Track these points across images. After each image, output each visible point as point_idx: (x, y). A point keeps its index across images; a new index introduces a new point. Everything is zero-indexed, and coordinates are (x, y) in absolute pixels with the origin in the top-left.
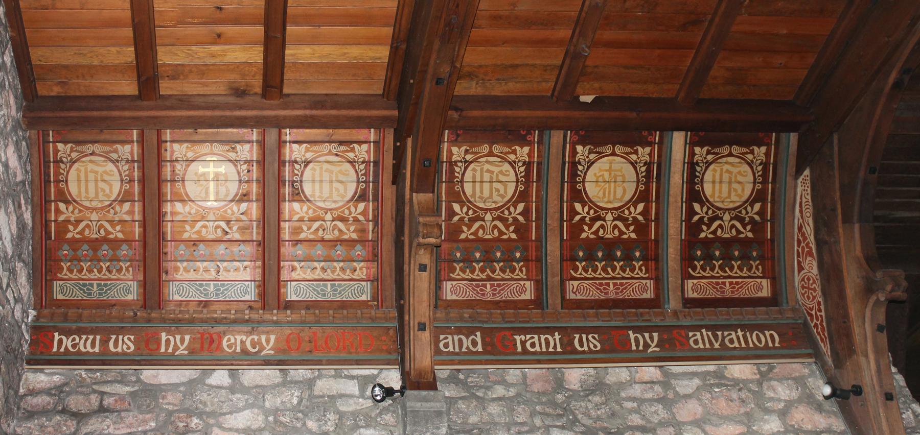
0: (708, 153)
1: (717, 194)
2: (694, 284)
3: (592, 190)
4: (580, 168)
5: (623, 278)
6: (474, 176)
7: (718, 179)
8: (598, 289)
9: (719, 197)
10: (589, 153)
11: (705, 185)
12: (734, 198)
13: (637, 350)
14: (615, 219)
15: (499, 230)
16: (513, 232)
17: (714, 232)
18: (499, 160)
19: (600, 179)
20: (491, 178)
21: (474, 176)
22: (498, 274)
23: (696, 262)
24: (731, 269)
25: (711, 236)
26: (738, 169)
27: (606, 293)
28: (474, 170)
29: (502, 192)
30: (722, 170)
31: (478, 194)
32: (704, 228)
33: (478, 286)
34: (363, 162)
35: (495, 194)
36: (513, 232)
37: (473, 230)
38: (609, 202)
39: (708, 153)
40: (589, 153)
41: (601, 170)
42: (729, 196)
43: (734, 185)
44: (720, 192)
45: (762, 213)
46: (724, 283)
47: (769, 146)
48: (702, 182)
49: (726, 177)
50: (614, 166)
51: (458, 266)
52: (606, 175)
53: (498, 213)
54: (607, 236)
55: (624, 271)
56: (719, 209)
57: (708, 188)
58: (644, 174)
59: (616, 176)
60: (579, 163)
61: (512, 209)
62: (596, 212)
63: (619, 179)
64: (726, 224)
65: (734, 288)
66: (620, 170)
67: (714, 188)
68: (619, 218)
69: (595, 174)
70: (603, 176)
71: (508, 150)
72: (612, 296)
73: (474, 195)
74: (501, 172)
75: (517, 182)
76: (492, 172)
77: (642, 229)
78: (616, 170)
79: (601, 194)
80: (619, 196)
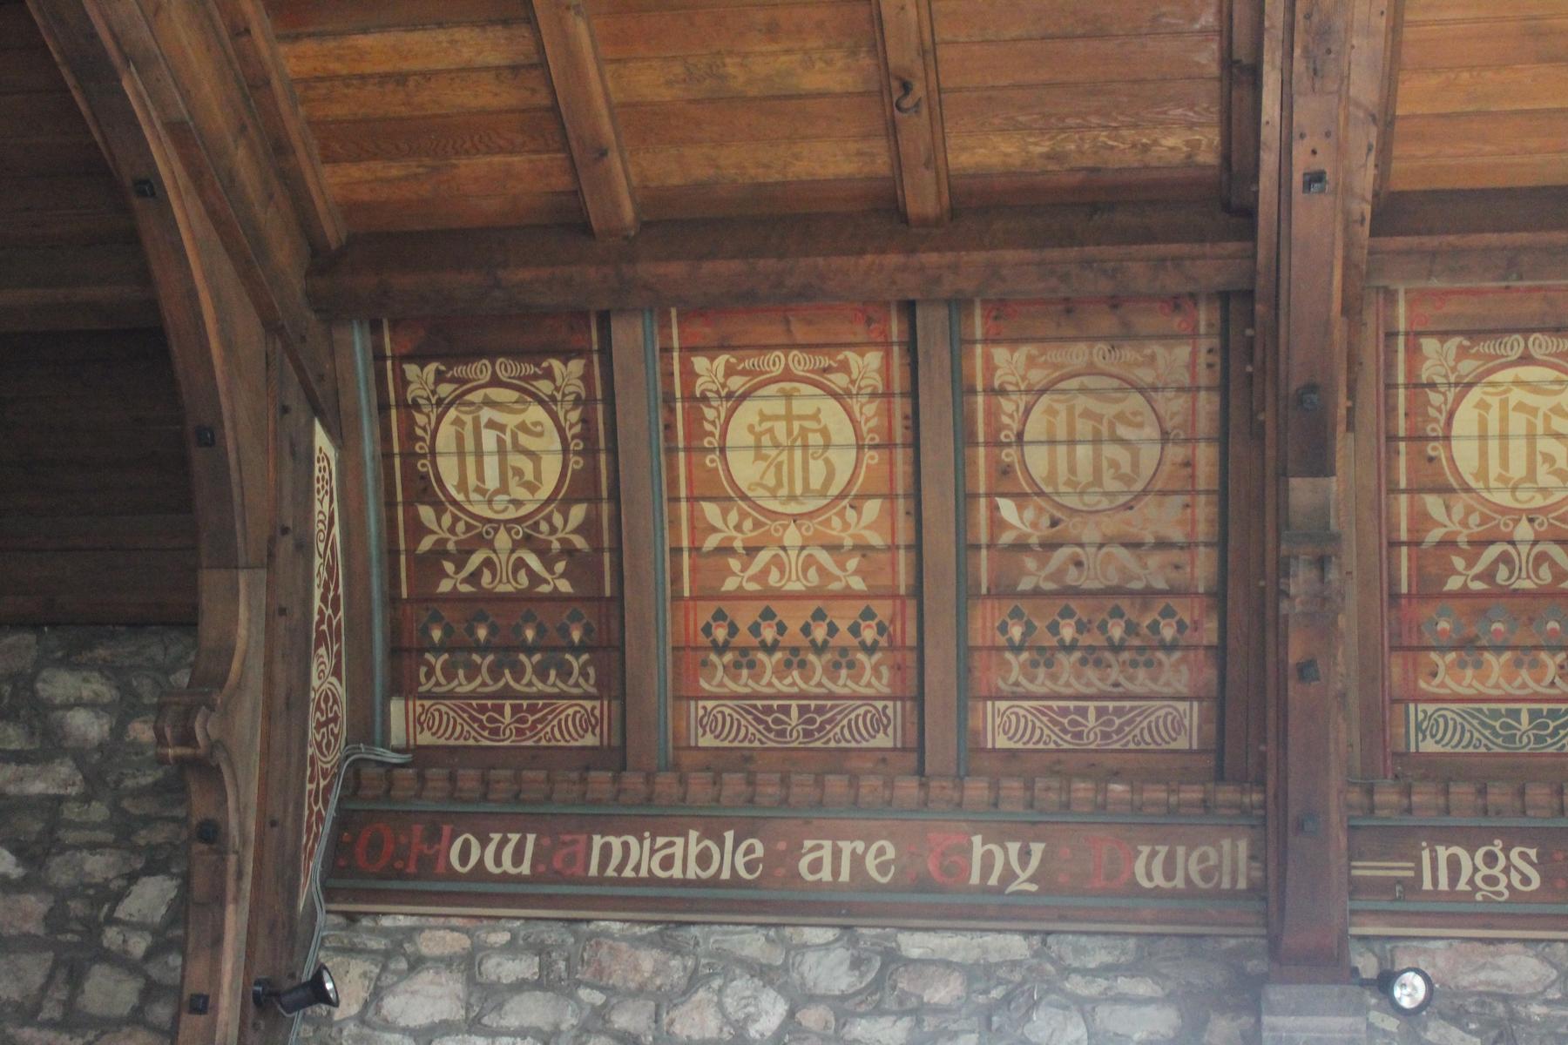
1: (1494, 468)
3: (744, 469)
4: (1435, 398)
5: (831, 696)
6: (460, 439)
7: (1061, 434)
8: (1055, 723)
9: (1501, 478)
10: (1458, 359)
11: (440, 461)
12: (1111, 484)
13: (1435, 893)
14: (516, 545)
15: (531, 573)
16: (562, 576)
18: (515, 395)
19: (766, 440)
20: (500, 441)
21: (460, 439)
22: (530, 682)
23: (522, 657)
24: (518, 674)
25: (465, 588)
27: (1078, 735)
28: (458, 422)
29: (529, 475)
30: (476, 422)
31: (472, 480)
32: (449, 567)
33: (483, 709)
34: (873, 395)
35: (513, 482)
36: (562, 576)
37: (755, 568)
38: (792, 497)
40: (1458, 359)
41: (764, 418)
42: (504, 488)
44: (1504, 462)
45: (588, 528)
47: (886, 345)
48: (433, 453)
49: (1518, 423)
50: (799, 407)
51: (439, 662)
52: (780, 428)
53: (813, 525)
54: (502, 588)
55: (834, 679)
56: (1504, 510)
57: (1465, 454)
58: (577, 429)
59: (804, 431)
60: (416, 406)
61: (558, 519)
62: (1485, 519)
63: (815, 439)
64: (503, 559)
65: (812, 721)
66: (815, 417)
67: (1483, 454)
68: (528, 541)
69: (751, 428)
70: (770, 431)
71: (532, 369)
72: (1092, 742)
73: (1052, 476)
74: (523, 427)
75: (565, 450)
76: (501, 428)
77: (581, 565)
78: (800, 418)
79: (771, 481)
80: (816, 482)
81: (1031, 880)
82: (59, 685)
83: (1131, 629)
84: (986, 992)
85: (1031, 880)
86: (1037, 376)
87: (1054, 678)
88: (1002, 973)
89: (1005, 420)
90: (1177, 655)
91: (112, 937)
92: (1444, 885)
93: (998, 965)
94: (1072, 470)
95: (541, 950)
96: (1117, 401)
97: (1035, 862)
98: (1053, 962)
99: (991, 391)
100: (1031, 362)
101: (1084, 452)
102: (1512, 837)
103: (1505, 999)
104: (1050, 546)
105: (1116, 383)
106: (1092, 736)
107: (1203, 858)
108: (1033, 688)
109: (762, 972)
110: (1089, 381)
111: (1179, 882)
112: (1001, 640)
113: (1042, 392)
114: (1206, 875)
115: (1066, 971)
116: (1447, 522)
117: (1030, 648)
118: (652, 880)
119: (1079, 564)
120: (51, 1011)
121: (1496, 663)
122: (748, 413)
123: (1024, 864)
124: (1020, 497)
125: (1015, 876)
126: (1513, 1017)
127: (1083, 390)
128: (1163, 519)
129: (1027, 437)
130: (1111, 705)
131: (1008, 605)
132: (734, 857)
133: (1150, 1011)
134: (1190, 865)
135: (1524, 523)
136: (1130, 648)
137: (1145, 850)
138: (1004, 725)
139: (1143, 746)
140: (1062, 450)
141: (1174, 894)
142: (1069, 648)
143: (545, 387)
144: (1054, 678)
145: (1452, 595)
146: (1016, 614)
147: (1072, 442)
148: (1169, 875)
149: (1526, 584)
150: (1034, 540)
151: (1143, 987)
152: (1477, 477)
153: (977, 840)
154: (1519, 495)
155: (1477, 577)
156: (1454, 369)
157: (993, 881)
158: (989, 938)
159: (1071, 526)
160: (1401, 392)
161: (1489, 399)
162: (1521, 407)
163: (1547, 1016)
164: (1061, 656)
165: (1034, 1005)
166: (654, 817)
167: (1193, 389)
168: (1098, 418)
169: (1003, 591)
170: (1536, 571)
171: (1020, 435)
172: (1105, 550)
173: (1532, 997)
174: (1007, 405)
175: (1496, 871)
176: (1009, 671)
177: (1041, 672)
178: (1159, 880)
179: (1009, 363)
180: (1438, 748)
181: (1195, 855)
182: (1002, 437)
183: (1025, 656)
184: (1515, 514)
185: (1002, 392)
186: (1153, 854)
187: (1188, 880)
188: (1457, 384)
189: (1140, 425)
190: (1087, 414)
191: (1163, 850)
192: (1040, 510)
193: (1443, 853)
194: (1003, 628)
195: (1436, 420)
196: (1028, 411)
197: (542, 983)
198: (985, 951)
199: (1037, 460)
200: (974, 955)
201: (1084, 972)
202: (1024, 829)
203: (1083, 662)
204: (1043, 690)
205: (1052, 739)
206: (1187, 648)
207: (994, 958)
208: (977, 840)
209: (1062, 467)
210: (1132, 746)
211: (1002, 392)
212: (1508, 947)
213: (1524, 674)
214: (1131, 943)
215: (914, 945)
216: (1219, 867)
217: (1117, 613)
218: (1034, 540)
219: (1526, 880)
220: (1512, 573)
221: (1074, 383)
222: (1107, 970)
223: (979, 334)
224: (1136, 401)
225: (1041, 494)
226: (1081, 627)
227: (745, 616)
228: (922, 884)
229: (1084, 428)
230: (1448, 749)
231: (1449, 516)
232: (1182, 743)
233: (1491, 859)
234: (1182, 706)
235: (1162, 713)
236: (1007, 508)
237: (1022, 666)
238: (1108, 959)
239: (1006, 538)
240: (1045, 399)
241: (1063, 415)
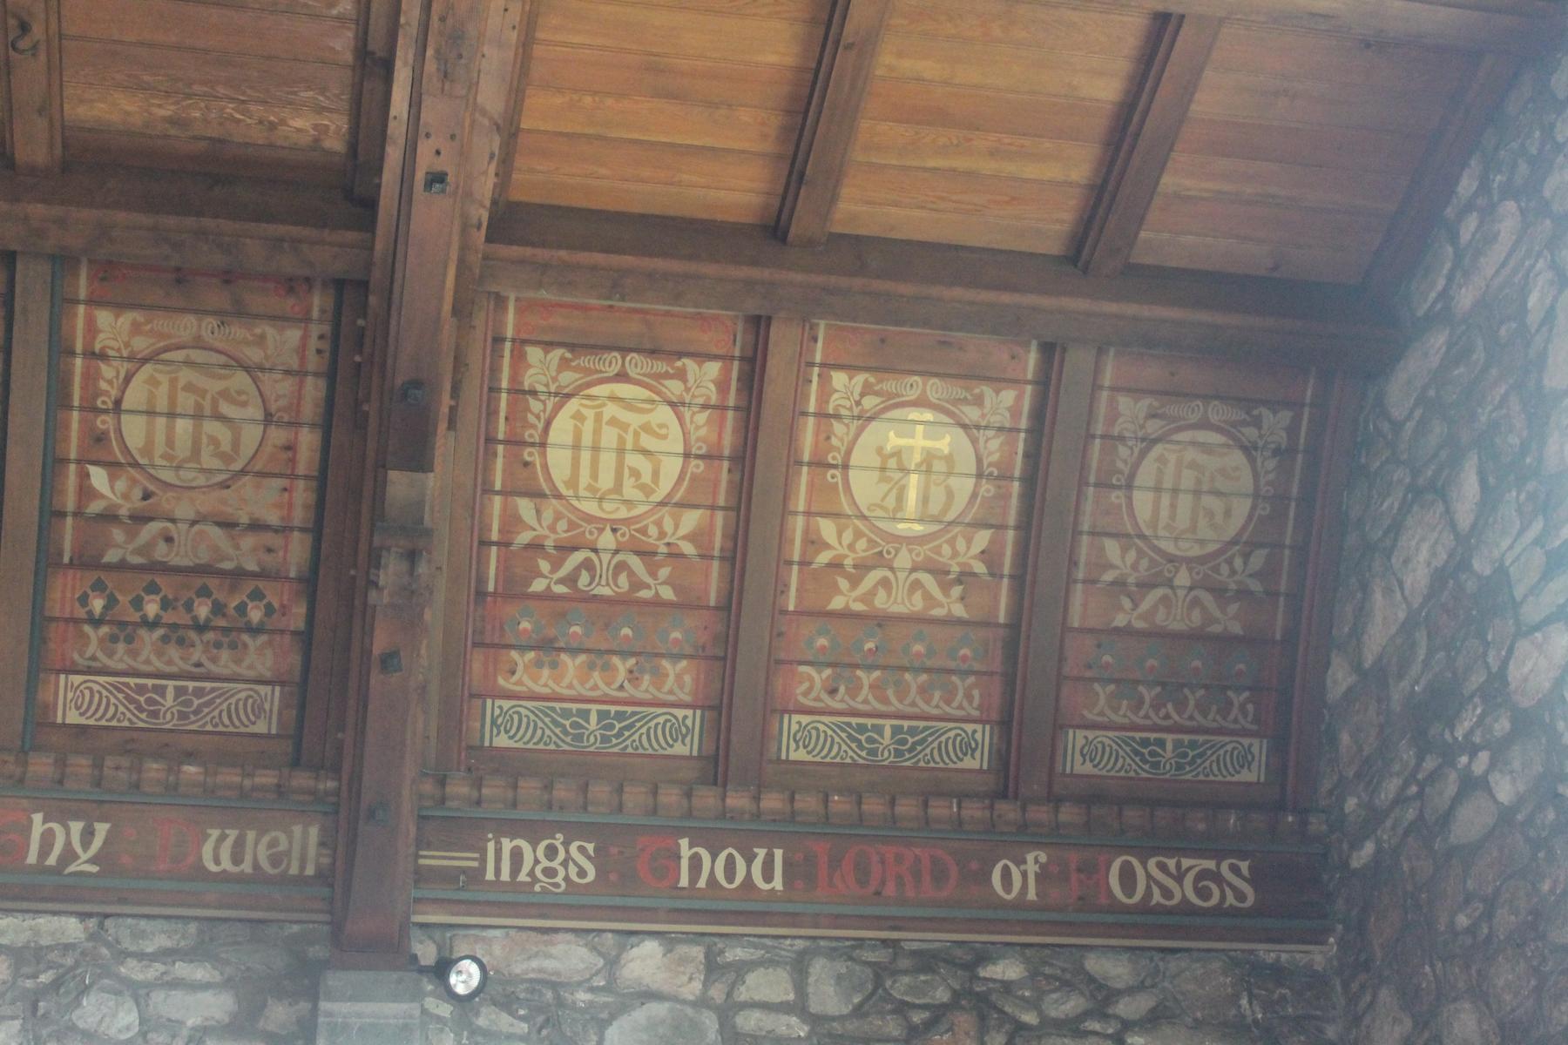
0: (867, 390)
2: (503, 713)
4: (535, 405)
7: (162, 405)
9: (590, 488)
10: (560, 370)
13: (498, 882)
17: (868, 598)
26: (644, 418)
39: (867, 390)
40: (560, 370)
43: (633, 460)
46: (879, 730)
49: (609, 437)
56: (590, 519)
57: (558, 461)
62: (572, 526)
81: (91, 861)
83: (218, 609)
84: (35, 976)
85: (91, 861)
86: (141, 344)
87: (134, 654)
88: (53, 956)
89: (103, 385)
90: (264, 638)
92: (505, 876)
93: (50, 948)
94: (170, 442)
96: (221, 377)
97: (97, 843)
98: (108, 945)
99: (90, 354)
100: (136, 329)
101: (183, 426)
102: (574, 831)
103: (554, 986)
104: (140, 519)
105: (223, 359)
106: (169, 716)
107: (273, 844)
108: (112, 664)
110: (197, 355)
111: (247, 867)
112: (81, 613)
113: (145, 361)
114: (275, 861)
115: (124, 955)
116: (537, 526)
117: (110, 622)
119: (169, 539)
121: (572, 665)
123: (86, 844)
124: (112, 466)
125: (76, 857)
126: (560, 1003)
127: (189, 363)
129: (125, 406)
130: (191, 685)
131: (94, 576)
133: (207, 997)
134: (259, 850)
135: (608, 533)
136: (215, 628)
137: (215, 833)
138: (74, 700)
139: (220, 728)
140: (161, 422)
141: (240, 879)
142: (153, 625)
144: (134, 654)
145: (537, 597)
146: (99, 586)
147: (172, 415)
148: (237, 859)
149: (606, 591)
150: (123, 512)
151: (201, 973)
152: (568, 484)
153: (38, 818)
154: (607, 506)
155: (561, 581)
156: (555, 379)
157: (52, 860)
158: (42, 921)
159: (165, 501)
160: (504, 396)
161: (584, 411)
162: (613, 422)
163: (591, 1004)
164: (143, 632)
165: (84, 990)
167: (301, 373)
168: (202, 393)
169: (87, 561)
170: (616, 575)
171: (118, 403)
172: (197, 527)
173: (579, 984)
174: (107, 371)
175: (555, 864)
176: (87, 645)
177: (121, 647)
178: (226, 864)
179: (112, 328)
180: (511, 744)
181: (266, 839)
182: (99, 403)
183: (105, 630)
184: (599, 523)
185: (103, 356)
186: (223, 838)
187: (256, 866)
188: (556, 394)
189: (244, 404)
190: (189, 387)
191: (233, 834)
192: (134, 481)
193: (507, 845)
194: (84, 600)
195: (534, 427)
196: (128, 379)
198: (36, 932)
199: (134, 430)
200: (21, 939)
201: (140, 956)
202: (88, 810)
203: (165, 639)
204: (121, 666)
205: (127, 717)
206: (273, 632)
207: (45, 941)
208: (38, 818)
209: (160, 438)
210: (209, 728)
211: (103, 356)
212: (560, 936)
213: (596, 676)
214: (192, 928)
216: (288, 853)
217: (204, 592)
218: (123, 512)
219: (582, 873)
220: (593, 578)
221: (178, 355)
223: (83, 293)
224: (241, 380)
225: (136, 465)
226: (166, 604)
229: (186, 402)
230: (520, 745)
231: (539, 520)
232: (261, 727)
233: (551, 852)
234: (264, 690)
235: (243, 695)
236: (99, 477)
237: (101, 641)
238: (169, 944)
239: (95, 507)
240: (148, 368)
241: (164, 389)
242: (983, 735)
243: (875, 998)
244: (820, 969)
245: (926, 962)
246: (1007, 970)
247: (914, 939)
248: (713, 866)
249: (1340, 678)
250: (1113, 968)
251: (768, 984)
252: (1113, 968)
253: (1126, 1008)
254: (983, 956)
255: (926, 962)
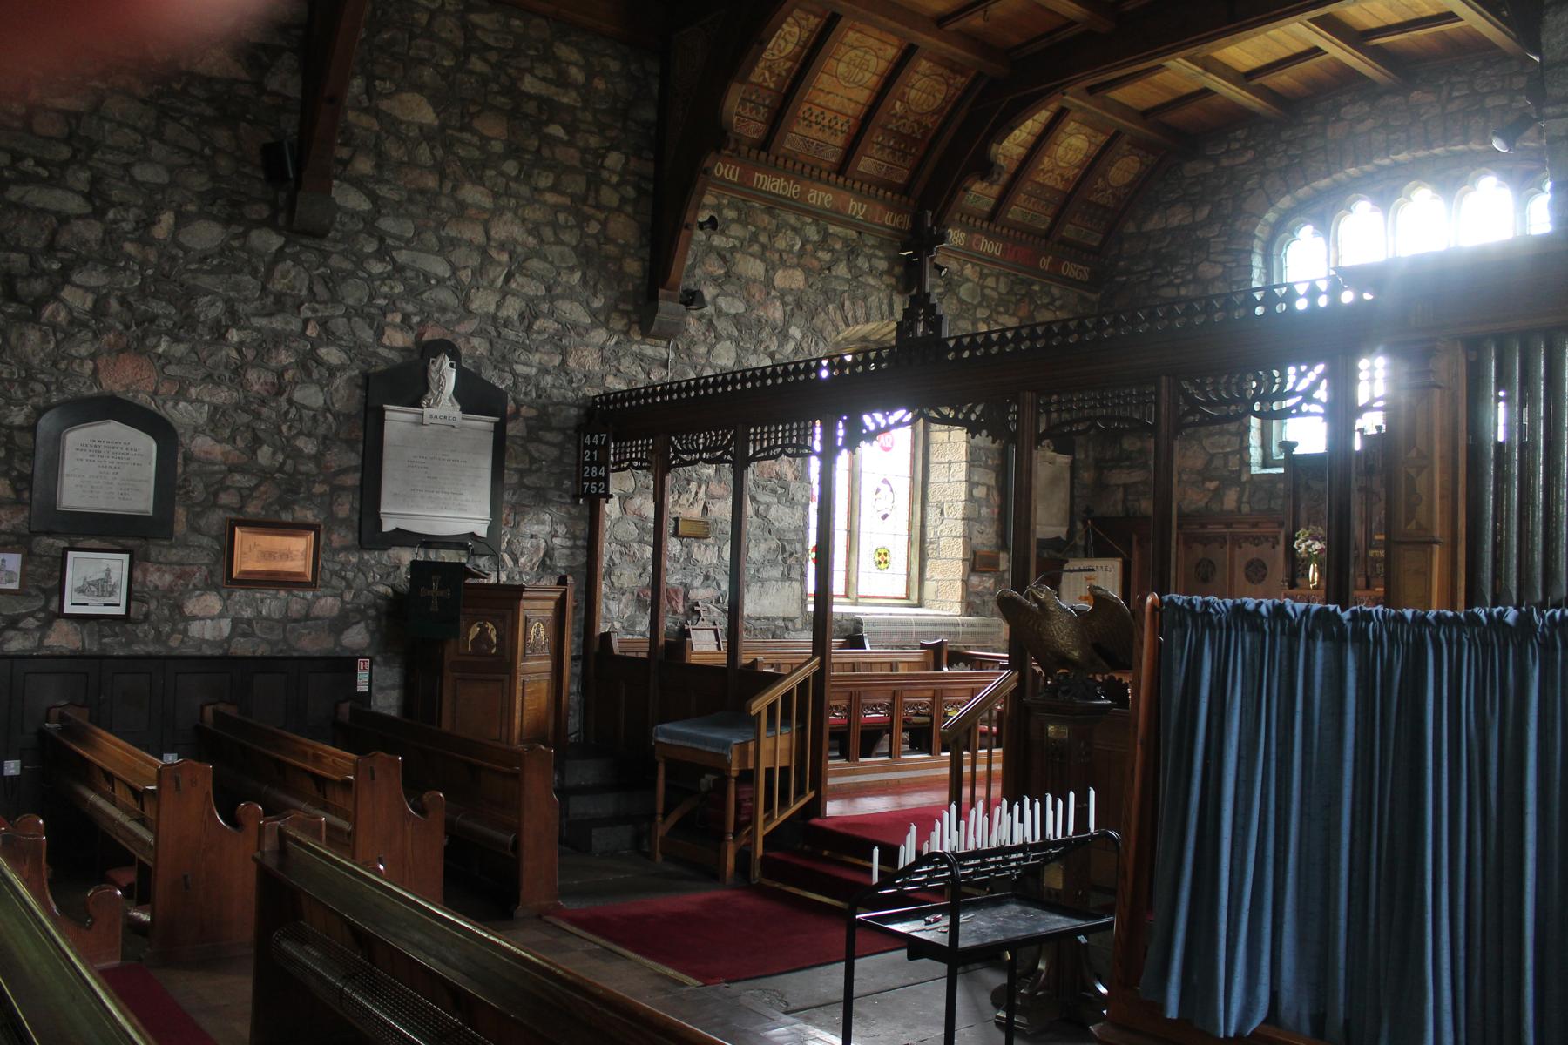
50: (868, 57)
82: (563, 51)
91: (605, 174)
95: (739, 210)
109: (794, 229)
118: (770, 193)
120: (591, 201)
122: (853, 53)
128: (928, 121)
132: (792, 190)
143: (804, 23)
151: (880, 254)
166: (774, 169)
169: (884, 127)
197: (738, 221)
215: (832, 229)
222: (873, 247)
224: (944, 88)
227: (816, 111)
228: (837, 212)
242: (1049, 220)
243: (1011, 291)
244: (1002, 279)
245: (1023, 282)
246: (1036, 288)
247: (1021, 275)
248: (988, 246)
249: (1131, 228)
250: (1056, 291)
251: (990, 282)
252: (1056, 291)
253: (1058, 303)
254: (1033, 283)
255: (1023, 282)
